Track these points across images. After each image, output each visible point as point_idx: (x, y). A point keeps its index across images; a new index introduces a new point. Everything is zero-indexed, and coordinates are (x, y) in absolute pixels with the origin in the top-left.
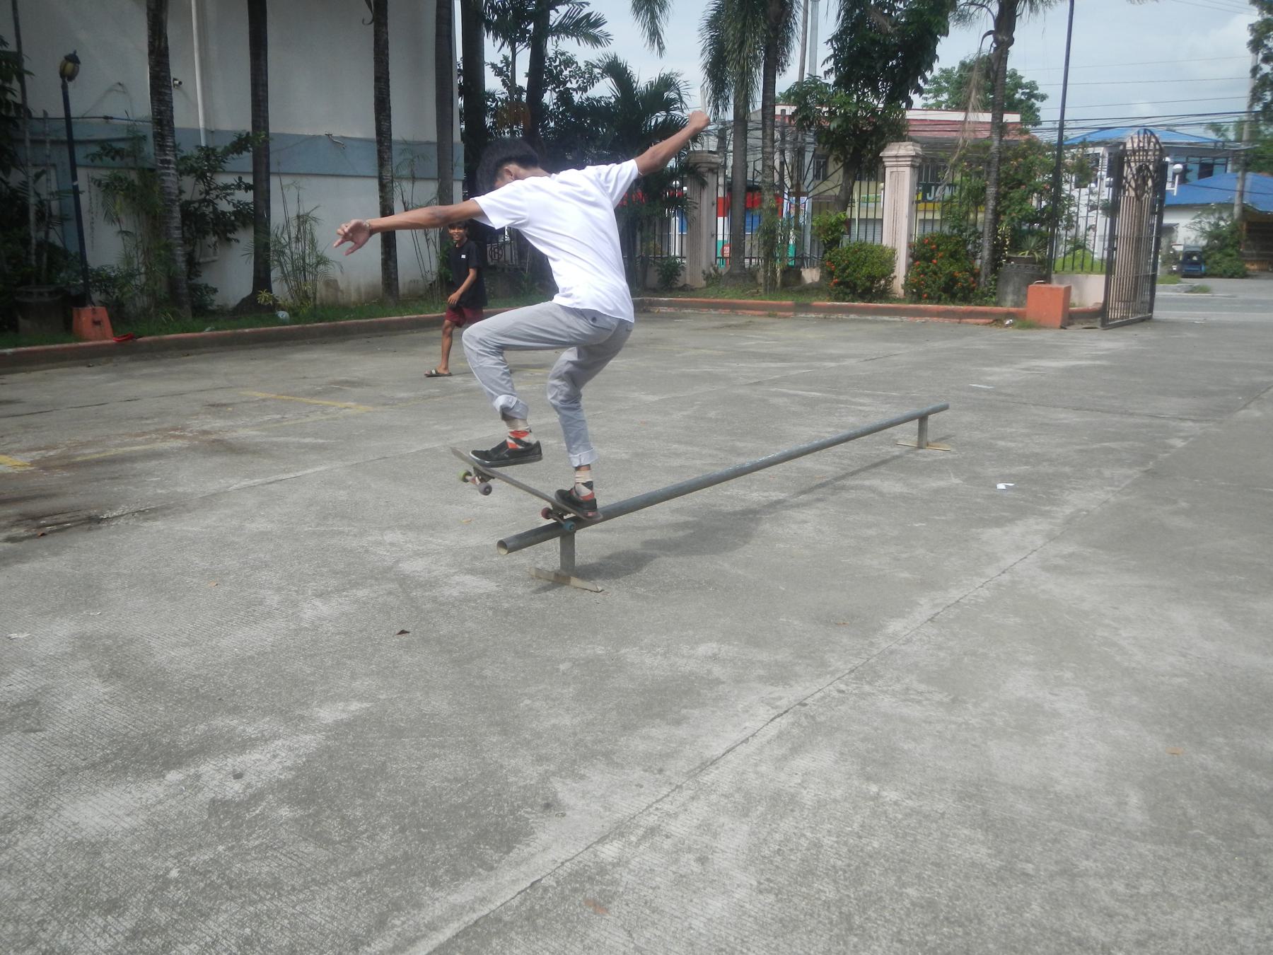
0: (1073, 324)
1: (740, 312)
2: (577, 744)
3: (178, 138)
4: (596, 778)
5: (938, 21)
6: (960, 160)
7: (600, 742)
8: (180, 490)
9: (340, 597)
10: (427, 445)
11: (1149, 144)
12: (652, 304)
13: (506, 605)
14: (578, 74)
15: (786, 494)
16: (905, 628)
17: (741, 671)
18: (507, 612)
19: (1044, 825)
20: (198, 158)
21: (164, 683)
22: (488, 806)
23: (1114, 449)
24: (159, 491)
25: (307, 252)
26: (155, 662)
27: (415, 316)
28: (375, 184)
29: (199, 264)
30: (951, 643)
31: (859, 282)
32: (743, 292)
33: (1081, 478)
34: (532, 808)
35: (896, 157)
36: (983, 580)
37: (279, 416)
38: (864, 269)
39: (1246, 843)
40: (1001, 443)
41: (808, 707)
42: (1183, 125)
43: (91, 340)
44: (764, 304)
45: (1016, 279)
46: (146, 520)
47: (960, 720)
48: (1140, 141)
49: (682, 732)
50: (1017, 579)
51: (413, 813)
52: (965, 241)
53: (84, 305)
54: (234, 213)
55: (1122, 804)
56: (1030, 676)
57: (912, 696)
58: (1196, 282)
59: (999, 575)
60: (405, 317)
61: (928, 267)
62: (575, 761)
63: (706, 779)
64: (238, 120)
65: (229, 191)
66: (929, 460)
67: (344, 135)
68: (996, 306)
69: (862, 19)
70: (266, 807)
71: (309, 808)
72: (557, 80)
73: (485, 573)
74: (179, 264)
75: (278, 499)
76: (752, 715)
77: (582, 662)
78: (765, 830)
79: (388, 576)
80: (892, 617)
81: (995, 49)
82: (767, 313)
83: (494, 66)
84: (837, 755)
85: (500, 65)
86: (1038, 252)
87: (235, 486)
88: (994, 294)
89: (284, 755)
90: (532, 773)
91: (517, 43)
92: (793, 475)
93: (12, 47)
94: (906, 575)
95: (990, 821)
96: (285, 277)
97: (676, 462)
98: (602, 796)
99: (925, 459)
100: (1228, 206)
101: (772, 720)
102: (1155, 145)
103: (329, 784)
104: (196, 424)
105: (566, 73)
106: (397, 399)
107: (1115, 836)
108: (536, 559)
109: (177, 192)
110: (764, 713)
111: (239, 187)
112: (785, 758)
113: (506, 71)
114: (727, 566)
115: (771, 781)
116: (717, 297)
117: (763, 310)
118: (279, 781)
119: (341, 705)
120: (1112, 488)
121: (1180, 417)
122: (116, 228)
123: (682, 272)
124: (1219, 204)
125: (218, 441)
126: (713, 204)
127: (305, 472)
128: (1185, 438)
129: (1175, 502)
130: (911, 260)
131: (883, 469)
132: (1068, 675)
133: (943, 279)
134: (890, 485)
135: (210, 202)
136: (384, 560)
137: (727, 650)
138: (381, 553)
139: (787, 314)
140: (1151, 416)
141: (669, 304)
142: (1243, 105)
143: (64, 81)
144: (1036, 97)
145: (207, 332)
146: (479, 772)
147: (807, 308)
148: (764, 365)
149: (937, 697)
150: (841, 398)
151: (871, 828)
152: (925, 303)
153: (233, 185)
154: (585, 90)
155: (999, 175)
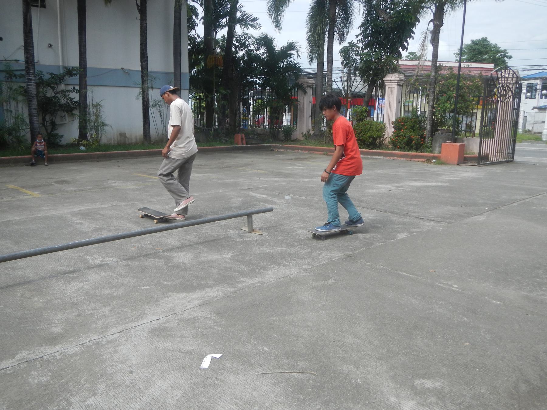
0: (468, 163)
3: (37, 68)
5: (409, 16)
10: (15, 218)
11: (509, 74)
12: (275, 147)
29: (56, 125)
35: (391, 80)
44: (322, 149)
45: (440, 140)
60: (143, 150)
61: (400, 133)
64: (74, 62)
67: (130, 69)
68: (431, 153)
72: (243, 45)
74: (35, 125)
88: (431, 147)
91: (217, 29)
102: (513, 75)
105: (247, 42)
116: (305, 145)
117: (322, 152)
123: (293, 133)
126: (310, 102)
140: (418, 218)
141: (281, 148)
144: (507, 57)
152: (397, 151)
153: (70, 90)
154: (258, 50)
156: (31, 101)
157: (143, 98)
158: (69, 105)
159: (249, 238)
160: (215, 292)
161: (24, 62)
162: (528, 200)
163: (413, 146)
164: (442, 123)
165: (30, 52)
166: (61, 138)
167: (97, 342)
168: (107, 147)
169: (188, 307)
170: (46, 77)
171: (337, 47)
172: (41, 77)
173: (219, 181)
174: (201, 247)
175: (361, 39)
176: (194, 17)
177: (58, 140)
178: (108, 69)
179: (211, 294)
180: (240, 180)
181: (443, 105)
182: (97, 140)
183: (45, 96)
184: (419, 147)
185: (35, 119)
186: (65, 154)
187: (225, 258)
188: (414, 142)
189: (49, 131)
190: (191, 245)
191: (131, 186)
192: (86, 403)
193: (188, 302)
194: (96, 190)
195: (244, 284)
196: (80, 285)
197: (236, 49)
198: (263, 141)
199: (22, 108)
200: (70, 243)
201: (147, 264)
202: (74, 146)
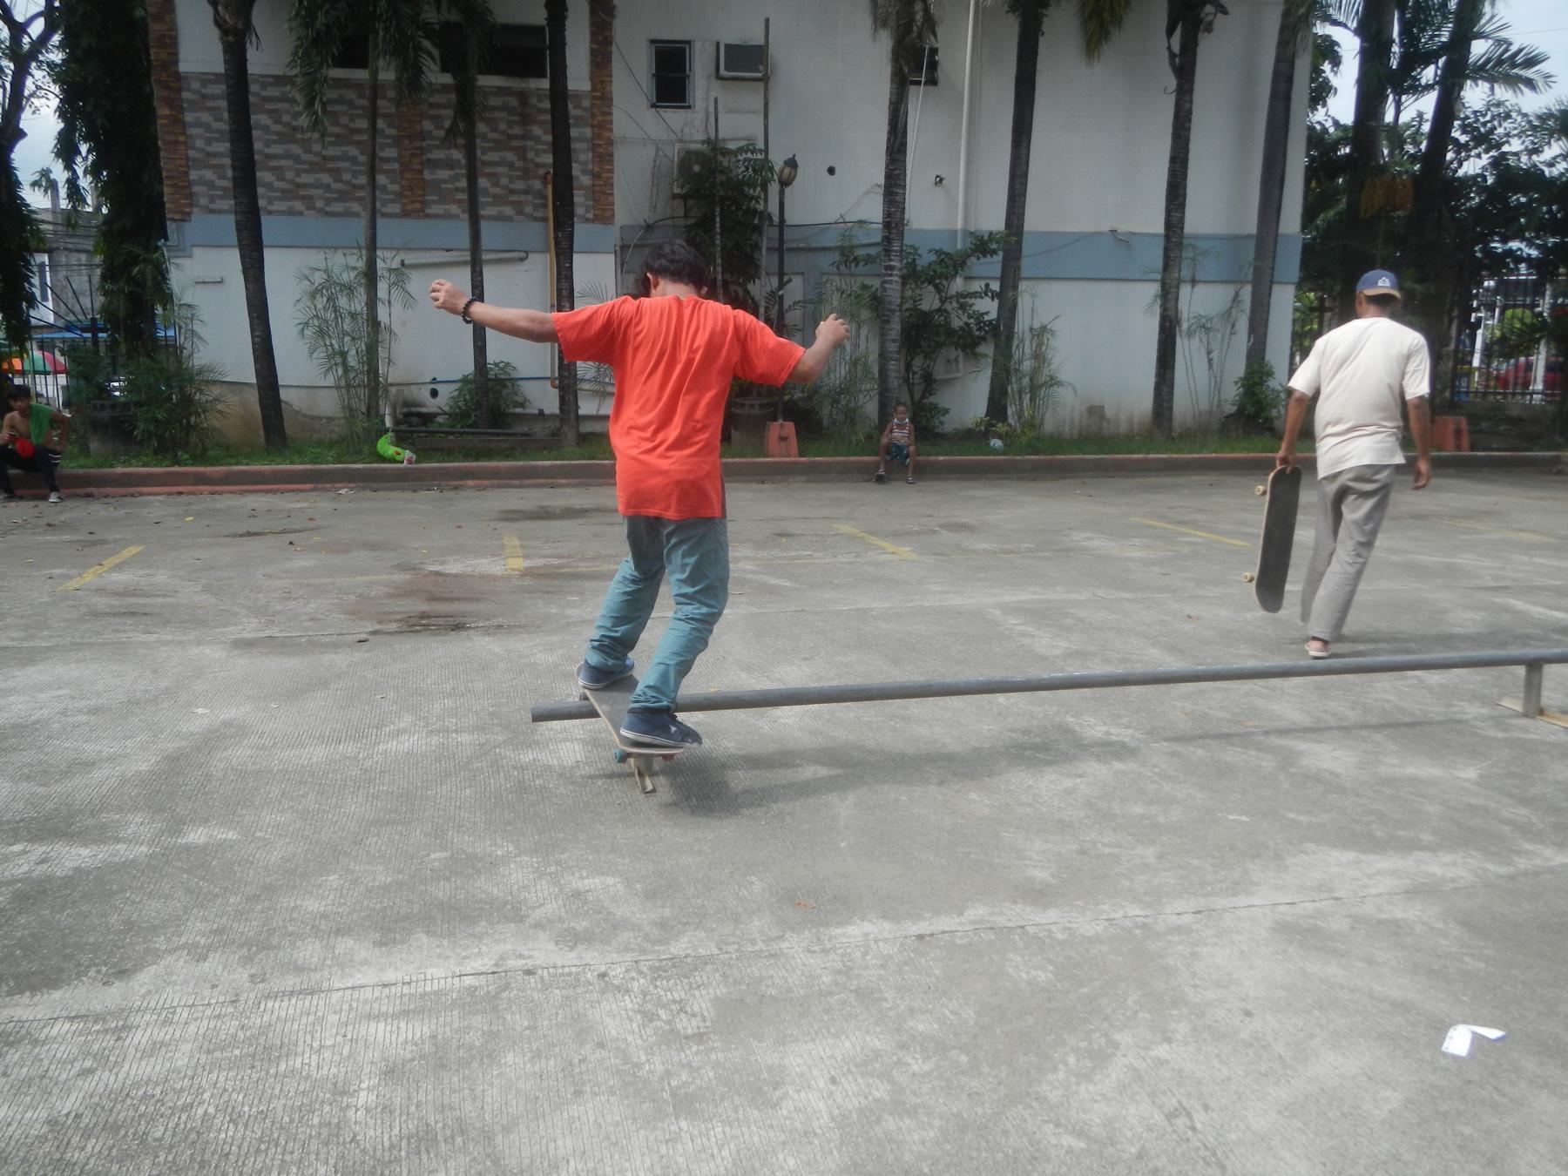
3: (908, 240)
10: (874, 605)
29: (935, 381)
43: (774, 456)
50: (1195, 927)
53: (775, 419)
59: (1178, 914)
60: (1151, 456)
64: (993, 220)
67: (1133, 230)
72: (1483, 139)
74: (890, 380)
93: (760, 157)
105: (1500, 131)
134: (1329, 757)
143: (782, 187)
153: (977, 292)
154: (1536, 151)
156: (888, 322)
157: (1164, 308)
158: (970, 332)
159: (1528, 732)
160: (1446, 865)
161: (881, 226)
166: (943, 415)
167: (1143, 923)
168: (1057, 443)
169: (1373, 891)
170: (925, 259)
172: (914, 260)
173: (1394, 558)
174: (1377, 737)
176: (1327, 67)
177: (936, 421)
178: (1074, 233)
179: (1437, 870)
180: (1465, 560)
182: (1033, 424)
183: (915, 309)
185: (892, 365)
187: (1459, 778)
189: (917, 396)
190: (1344, 728)
191: (1135, 551)
192: (1152, 1054)
193: (1370, 877)
194: (1046, 554)
195: (1538, 862)
196: (1068, 783)
197: (1458, 153)
198: (1532, 441)
199: (867, 339)
200: (1045, 676)
201: (1229, 759)
202: (973, 437)
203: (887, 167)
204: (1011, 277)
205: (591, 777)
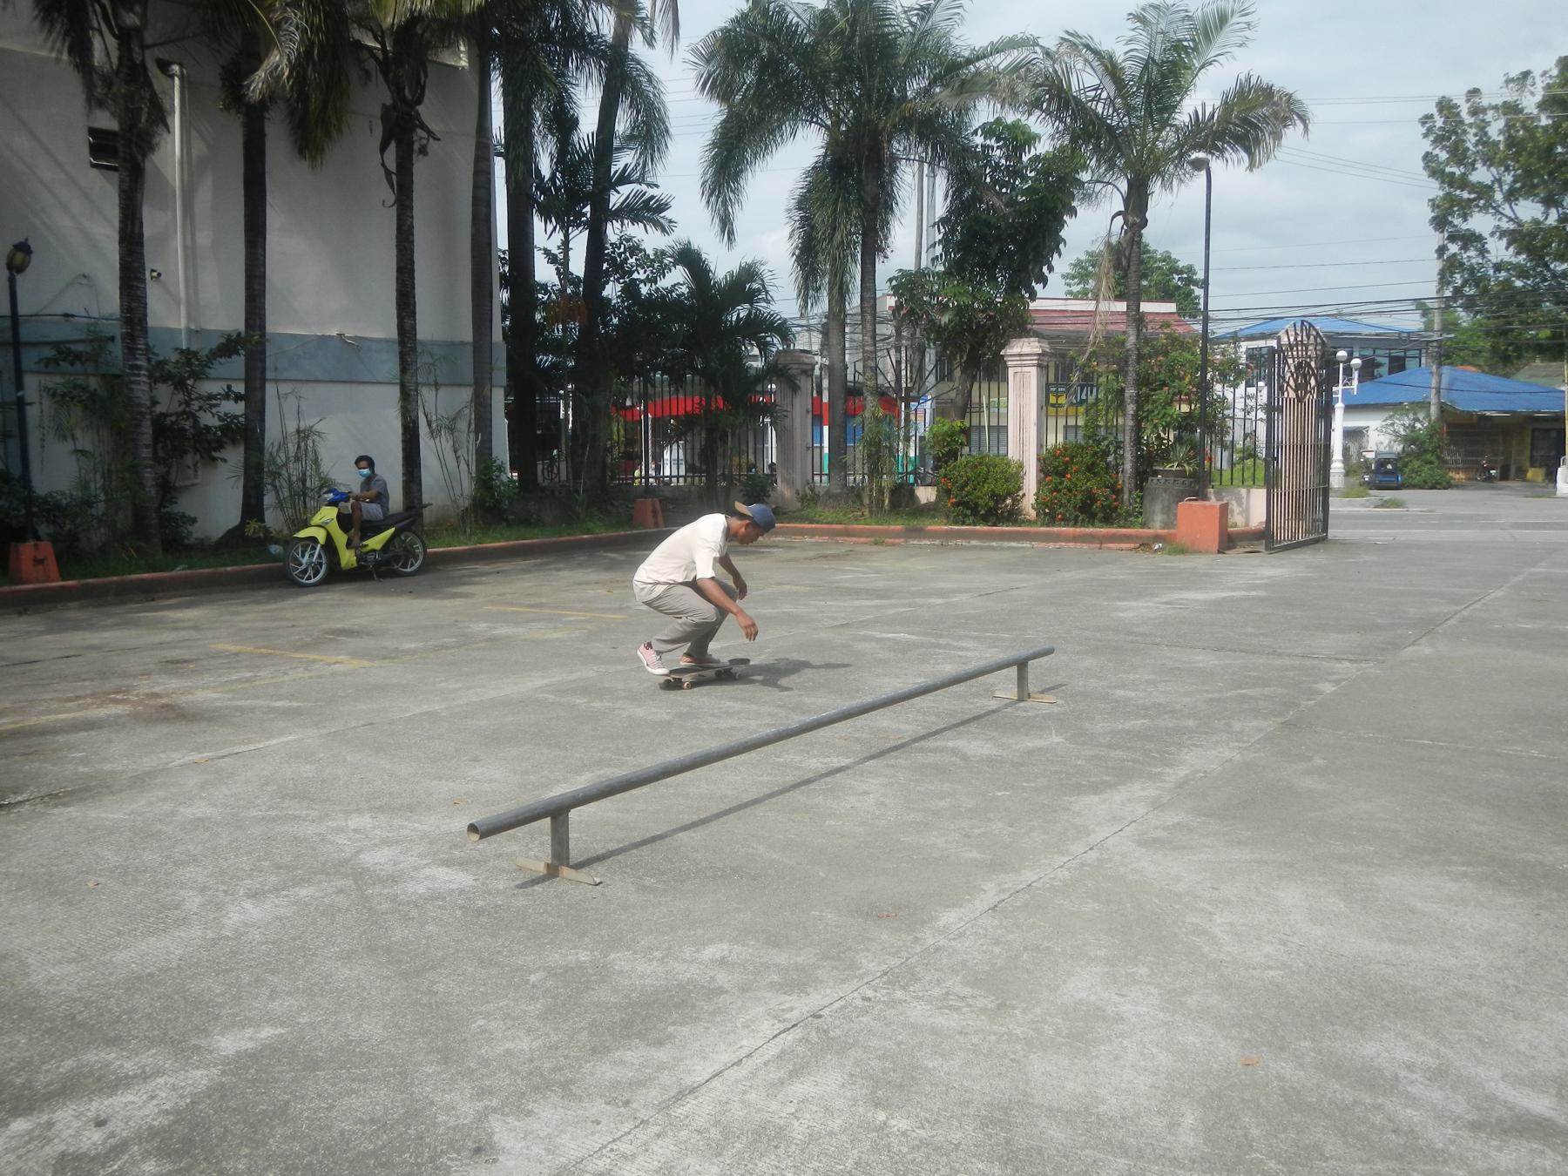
1: (840, 540)
2: (531, 1073)
4: (545, 1114)
6: (1089, 359)
7: (561, 1069)
8: (107, 767)
9: (277, 897)
10: (426, 708)
11: (1309, 338)
13: (481, 903)
14: (645, 262)
15: (851, 760)
16: (961, 919)
17: (751, 977)
18: (480, 912)
19: (1076, 1153)
20: (178, 362)
21: (34, 1009)
22: (404, 1152)
23: (1251, 697)
24: (81, 769)
25: (308, 473)
26: (29, 983)
27: (441, 549)
28: (394, 392)
29: (176, 488)
30: (1010, 937)
31: (981, 502)
32: (844, 515)
33: (1206, 733)
34: (458, 1154)
35: (1020, 355)
36: (1065, 859)
37: (251, 674)
38: (986, 486)
39: (1312, 1167)
40: (1119, 692)
41: (823, 1019)
42: (1360, 314)
46: (56, 806)
47: (1004, 1029)
48: (1296, 334)
49: (662, 1055)
51: (310, 1164)
52: (1104, 451)
53: (24, 540)
54: (220, 428)
55: (1173, 1126)
56: (1096, 973)
57: (951, 1003)
58: (1388, 495)
61: (1061, 483)
62: (524, 1094)
63: (679, 1111)
64: (228, 317)
65: (214, 402)
66: (1030, 714)
69: (976, 198)
70: (126, 1161)
71: (181, 1161)
72: (620, 269)
73: (463, 864)
74: (147, 489)
75: (228, 778)
76: (753, 1031)
77: (559, 971)
78: (739, 1171)
79: (343, 870)
80: (948, 906)
81: (1126, 231)
82: (872, 539)
83: (547, 252)
84: (846, 1077)
85: (555, 251)
86: (1189, 464)
87: (178, 762)
88: (1141, 513)
89: (164, 1095)
90: (467, 1109)
92: (864, 736)
94: (974, 854)
95: (1012, 1151)
96: (280, 505)
97: (724, 724)
98: (549, 1136)
99: (1025, 714)
100: (1425, 405)
101: (776, 1036)
103: (213, 1131)
104: (144, 686)
105: (632, 261)
106: (403, 651)
107: (1157, 1165)
108: (530, 846)
109: (148, 403)
110: (768, 1027)
111: (227, 396)
112: (782, 1083)
113: (560, 262)
114: (761, 848)
115: (758, 1110)
117: (867, 537)
118: (151, 1128)
119: (249, 1032)
120: (1241, 745)
121: (1337, 656)
122: (69, 446)
124: (1413, 403)
125: (168, 705)
126: (808, 412)
127: (267, 743)
128: (1337, 682)
129: (1311, 759)
130: (1042, 475)
131: (973, 727)
132: (1143, 971)
133: (1079, 497)
134: (975, 745)
135: (192, 415)
136: (343, 851)
137: (739, 952)
138: (340, 842)
139: (897, 541)
142: (1428, 288)
143: (11, 274)
145: (179, 572)
146: (402, 1111)
147: (918, 533)
148: (857, 603)
149: (981, 1002)
150: (942, 641)
151: (868, 1164)
153: (220, 394)
155: (1138, 375)
162: (1466, 613)
163: (1097, 514)
164: (1164, 455)
165: (139, 292)
171: (886, 270)
175: (941, 255)
181: (1163, 412)
184: (1109, 516)
186: (243, 567)
188: (1099, 503)
203: (122, 258)
204: (256, 378)
205: (519, 887)
